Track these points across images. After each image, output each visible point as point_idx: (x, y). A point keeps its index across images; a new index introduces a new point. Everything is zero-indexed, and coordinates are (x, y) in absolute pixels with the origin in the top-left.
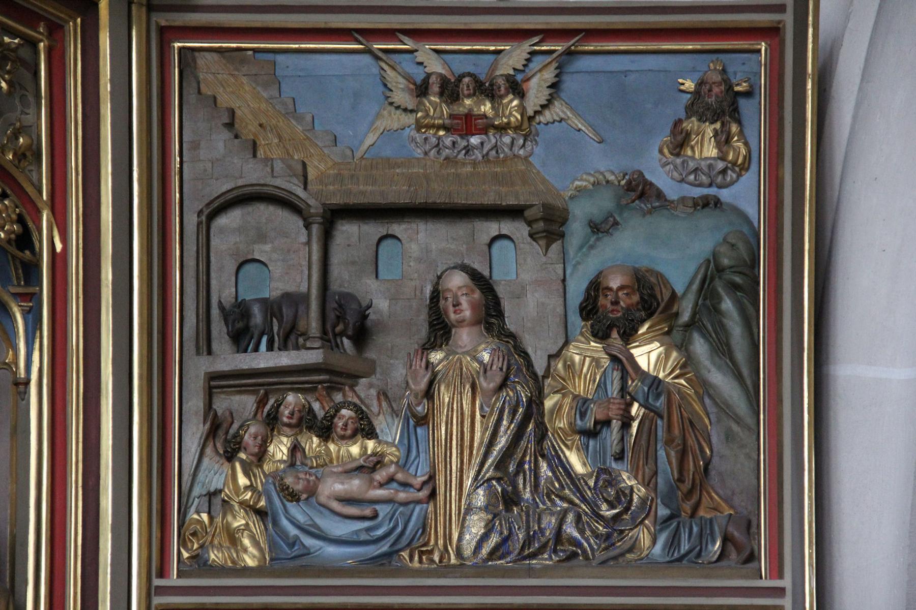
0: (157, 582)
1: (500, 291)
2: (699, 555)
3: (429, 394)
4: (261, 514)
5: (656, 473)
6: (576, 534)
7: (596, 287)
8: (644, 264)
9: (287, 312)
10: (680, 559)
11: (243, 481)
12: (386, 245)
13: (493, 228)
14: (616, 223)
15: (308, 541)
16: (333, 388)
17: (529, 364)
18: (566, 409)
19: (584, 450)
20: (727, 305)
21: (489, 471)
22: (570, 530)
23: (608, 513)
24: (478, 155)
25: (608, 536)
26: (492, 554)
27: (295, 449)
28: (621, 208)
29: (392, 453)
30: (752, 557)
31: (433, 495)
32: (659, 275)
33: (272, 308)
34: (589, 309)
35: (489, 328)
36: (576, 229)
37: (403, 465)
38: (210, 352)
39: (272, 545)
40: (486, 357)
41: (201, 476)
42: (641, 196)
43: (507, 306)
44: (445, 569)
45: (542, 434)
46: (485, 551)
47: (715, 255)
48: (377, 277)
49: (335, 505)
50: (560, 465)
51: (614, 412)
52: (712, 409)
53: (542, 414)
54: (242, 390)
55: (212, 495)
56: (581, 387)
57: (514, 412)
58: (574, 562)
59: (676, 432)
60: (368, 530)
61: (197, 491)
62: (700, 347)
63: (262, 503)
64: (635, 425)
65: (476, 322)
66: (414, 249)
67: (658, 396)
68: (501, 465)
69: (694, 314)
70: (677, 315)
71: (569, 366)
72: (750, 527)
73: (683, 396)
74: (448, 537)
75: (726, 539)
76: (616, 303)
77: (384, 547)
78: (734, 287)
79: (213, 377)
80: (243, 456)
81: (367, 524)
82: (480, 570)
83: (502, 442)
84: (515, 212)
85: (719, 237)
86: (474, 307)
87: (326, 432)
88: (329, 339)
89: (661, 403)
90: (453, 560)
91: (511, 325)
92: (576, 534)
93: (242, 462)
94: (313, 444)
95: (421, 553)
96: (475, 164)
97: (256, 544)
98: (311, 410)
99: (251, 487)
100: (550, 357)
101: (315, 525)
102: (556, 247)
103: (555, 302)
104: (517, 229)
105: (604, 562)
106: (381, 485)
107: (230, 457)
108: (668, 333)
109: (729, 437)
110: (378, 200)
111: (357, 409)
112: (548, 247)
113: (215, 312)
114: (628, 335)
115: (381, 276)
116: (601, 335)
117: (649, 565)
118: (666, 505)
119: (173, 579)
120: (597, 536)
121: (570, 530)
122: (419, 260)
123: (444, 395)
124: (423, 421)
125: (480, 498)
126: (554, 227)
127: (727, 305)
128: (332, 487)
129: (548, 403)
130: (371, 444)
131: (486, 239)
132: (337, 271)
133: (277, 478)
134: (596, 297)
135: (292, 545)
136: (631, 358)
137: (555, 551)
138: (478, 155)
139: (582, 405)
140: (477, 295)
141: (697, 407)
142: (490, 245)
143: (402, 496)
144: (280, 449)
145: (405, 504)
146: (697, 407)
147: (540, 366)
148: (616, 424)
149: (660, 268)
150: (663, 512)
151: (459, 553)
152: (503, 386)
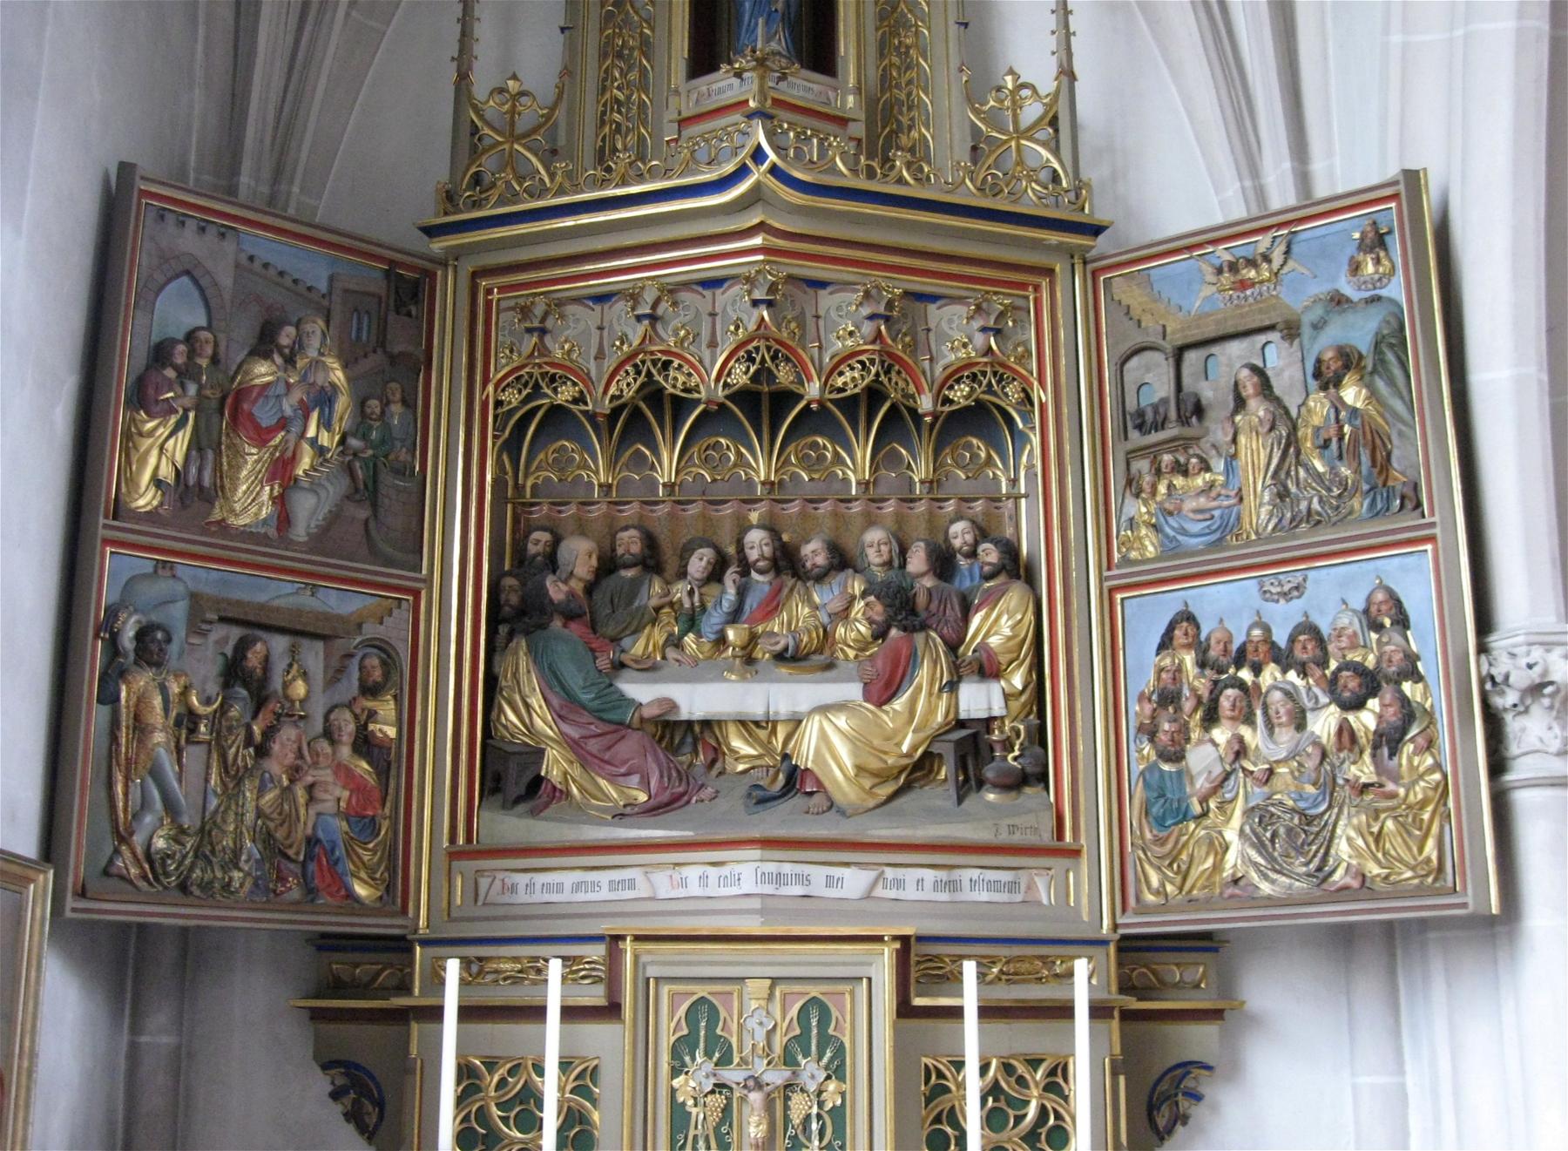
0: (1106, 574)
1: (1270, 373)
2: (1388, 509)
3: (1234, 441)
4: (1154, 526)
5: (1360, 464)
6: (1319, 509)
7: (1319, 361)
8: (1343, 342)
9: (1161, 410)
10: (1377, 514)
11: (1144, 510)
12: (1211, 360)
13: (1262, 339)
14: (1325, 322)
15: (1180, 537)
16: (1186, 449)
17: (1287, 412)
18: (1309, 436)
19: (1321, 457)
20: (1390, 357)
21: (1268, 481)
22: (1316, 505)
23: (1336, 492)
24: (1251, 300)
25: (1338, 507)
26: (1274, 529)
27: (1170, 486)
28: (1328, 312)
29: (1221, 478)
30: (1418, 505)
31: (1241, 500)
32: (1351, 347)
33: (1155, 408)
34: (1317, 374)
35: (1265, 396)
36: (1306, 331)
37: (1225, 485)
38: (1126, 438)
39: (1162, 545)
40: (1261, 413)
41: (1125, 510)
42: (1339, 303)
43: (1274, 382)
44: (1249, 543)
45: (1298, 453)
46: (1270, 527)
47: (1380, 328)
48: (1207, 378)
49: (1191, 515)
50: (1310, 470)
51: (1333, 432)
52: (1390, 419)
53: (1297, 441)
54: (1143, 457)
55: (1131, 519)
56: (1316, 420)
57: (1280, 444)
58: (1320, 526)
59: (1369, 437)
60: (1208, 527)
61: (1123, 519)
62: (1380, 384)
63: (1154, 521)
64: (1347, 437)
65: (1257, 395)
66: (1222, 359)
67: (1356, 418)
68: (1276, 473)
69: (1375, 365)
70: (1365, 367)
71: (1309, 411)
72: (1416, 487)
73: (1371, 417)
74: (1251, 523)
75: (1403, 498)
76: (1328, 368)
77: (1217, 535)
78: (1391, 346)
79: (1128, 453)
80: (1143, 495)
81: (1208, 523)
82: (1269, 539)
83: (1275, 462)
84: (1271, 328)
85: (1381, 317)
86: (1255, 386)
87: (1185, 473)
88: (1183, 420)
89: (1358, 422)
90: (1253, 537)
91: (1277, 391)
92: (1319, 509)
93: (1144, 500)
94: (1179, 481)
95: (1237, 536)
96: (1250, 305)
97: (1153, 544)
98: (1177, 462)
99: (1148, 512)
100: (1299, 407)
101: (1183, 528)
102: (1296, 342)
103: (1299, 375)
104: (1274, 336)
105: (1335, 524)
106: (1215, 499)
107: (1137, 496)
108: (1361, 379)
109: (1400, 434)
110: (1199, 338)
111: (1198, 456)
112: (1291, 344)
113: (1128, 417)
114: (1337, 382)
115: (1210, 377)
116: (1324, 388)
117: (1361, 521)
118: (1367, 483)
119: (1115, 572)
120: (1331, 508)
121: (1316, 505)
122: (1227, 365)
123: (1242, 439)
124: (1234, 456)
125: (1267, 498)
126: (1293, 332)
127: (1390, 357)
128: (1190, 504)
129: (1300, 434)
130: (1208, 476)
131: (1259, 346)
132: (1187, 380)
133: (1161, 503)
134: (1319, 368)
135: (1171, 542)
136: (1341, 399)
137: (1308, 522)
138: (1251, 300)
139: (1317, 430)
140: (1256, 379)
141: (1380, 420)
142: (1263, 348)
143: (1226, 503)
144: (1162, 489)
145: (1228, 507)
146: (1380, 420)
147: (1294, 413)
148: (1335, 440)
149: (1353, 343)
150: (1366, 487)
151: (1257, 533)
152: (1272, 429)
